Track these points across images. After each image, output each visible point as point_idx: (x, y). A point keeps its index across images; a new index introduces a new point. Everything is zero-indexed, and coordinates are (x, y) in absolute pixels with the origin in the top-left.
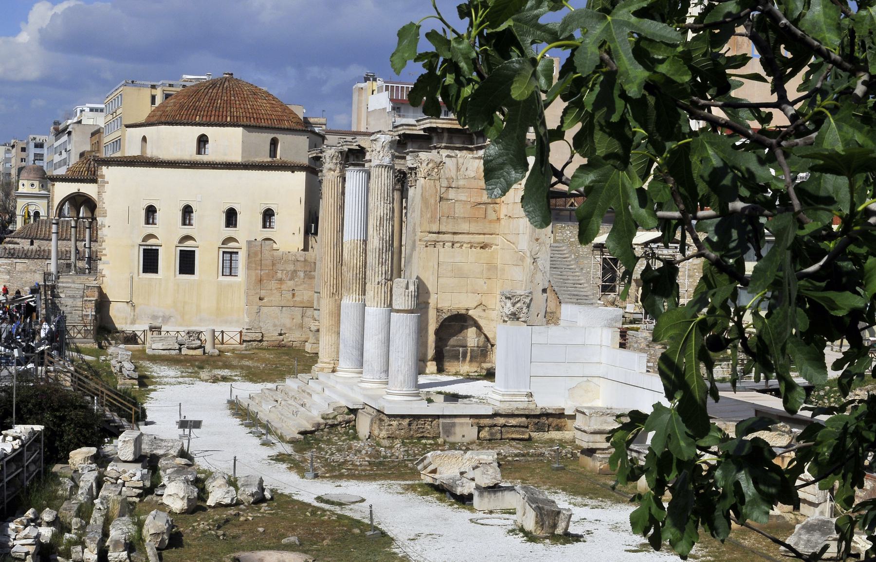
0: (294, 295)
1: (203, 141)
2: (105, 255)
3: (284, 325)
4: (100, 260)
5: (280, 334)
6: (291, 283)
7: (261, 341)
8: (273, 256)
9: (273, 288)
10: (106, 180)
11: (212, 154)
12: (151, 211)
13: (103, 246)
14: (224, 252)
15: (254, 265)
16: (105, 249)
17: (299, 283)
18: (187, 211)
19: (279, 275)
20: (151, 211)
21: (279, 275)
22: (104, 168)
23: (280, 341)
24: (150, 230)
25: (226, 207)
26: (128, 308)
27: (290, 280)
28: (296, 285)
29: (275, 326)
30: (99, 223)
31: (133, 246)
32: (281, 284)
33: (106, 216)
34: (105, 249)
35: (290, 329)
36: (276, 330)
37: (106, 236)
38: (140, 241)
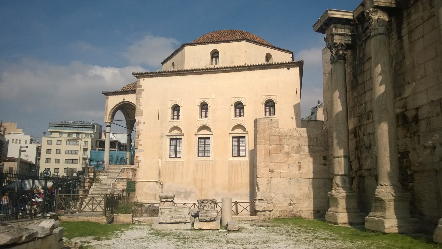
0: (300, 167)
1: (215, 54)
2: (141, 145)
3: (293, 196)
4: (136, 149)
5: (290, 205)
6: (297, 156)
7: (272, 211)
8: (279, 132)
9: (282, 161)
10: (142, 88)
11: (222, 64)
12: (176, 108)
13: (139, 138)
14: (233, 137)
15: (263, 141)
16: (140, 140)
17: (304, 156)
18: (204, 106)
19: (286, 149)
20: (176, 108)
21: (286, 149)
22: (141, 80)
23: (290, 211)
24: (176, 123)
25: (234, 101)
26: (158, 186)
27: (296, 153)
28: (301, 159)
29: (285, 196)
30: (137, 121)
31: (162, 137)
32: (288, 157)
33: (142, 116)
34: (140, 140)
35: (299, 199)
36: (285, 200)
37: (142, 130)
38: (167, 132)
